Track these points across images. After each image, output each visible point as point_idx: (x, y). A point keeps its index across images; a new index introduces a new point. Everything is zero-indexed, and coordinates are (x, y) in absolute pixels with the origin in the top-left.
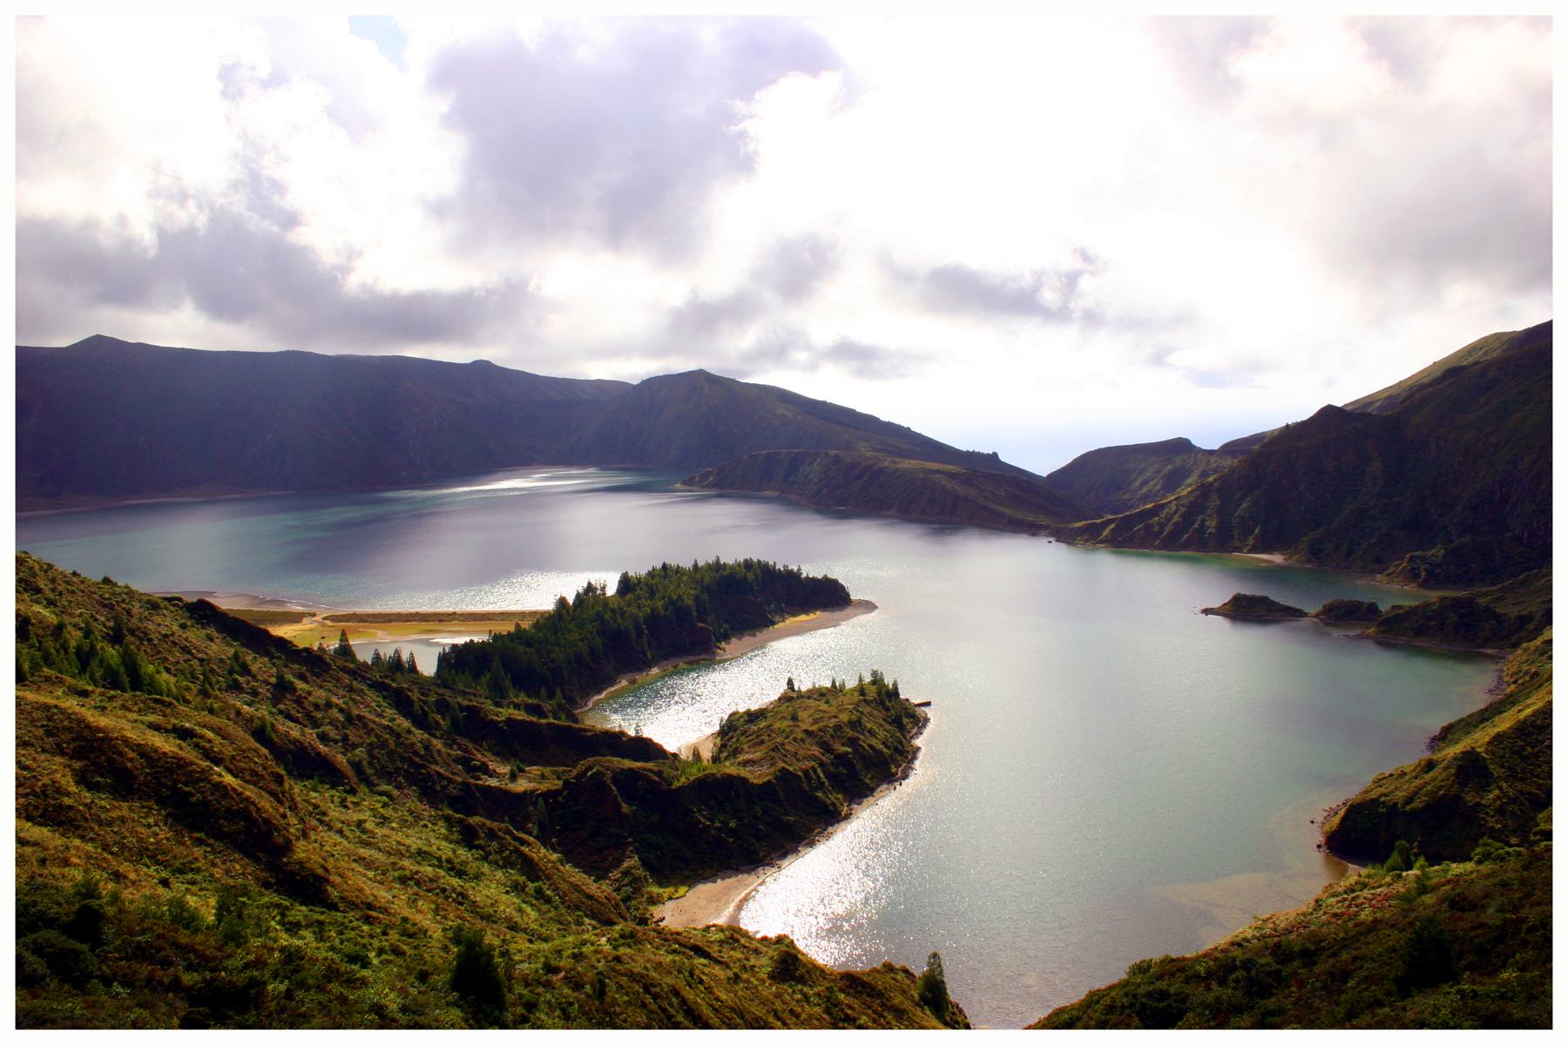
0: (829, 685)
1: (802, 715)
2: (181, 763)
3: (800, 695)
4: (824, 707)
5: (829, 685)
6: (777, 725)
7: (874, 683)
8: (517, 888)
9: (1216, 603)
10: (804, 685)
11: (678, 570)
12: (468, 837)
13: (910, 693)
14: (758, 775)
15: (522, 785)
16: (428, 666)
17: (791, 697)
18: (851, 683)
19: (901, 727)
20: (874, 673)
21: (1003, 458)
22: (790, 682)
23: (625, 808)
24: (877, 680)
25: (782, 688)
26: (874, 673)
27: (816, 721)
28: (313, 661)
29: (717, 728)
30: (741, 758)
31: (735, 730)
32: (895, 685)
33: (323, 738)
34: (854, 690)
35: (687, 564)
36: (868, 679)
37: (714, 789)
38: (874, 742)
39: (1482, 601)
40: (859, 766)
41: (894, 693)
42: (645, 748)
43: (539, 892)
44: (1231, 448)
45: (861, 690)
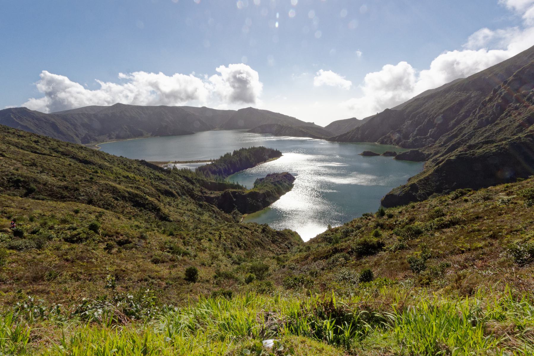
2: (137, 195)
8: (210, 216)
9: (360, 153)
11: (246, 149)
12: (201, 206)
15: (212, 196)
16: (194, 171)
21: (315, 124)
23: (235, 200)
28: (168, 172)
33: (170, 188)
35: (247, 148)
37: (253, 195)
39: (420, 151)
43: (216, 217)
44: (364, 119)
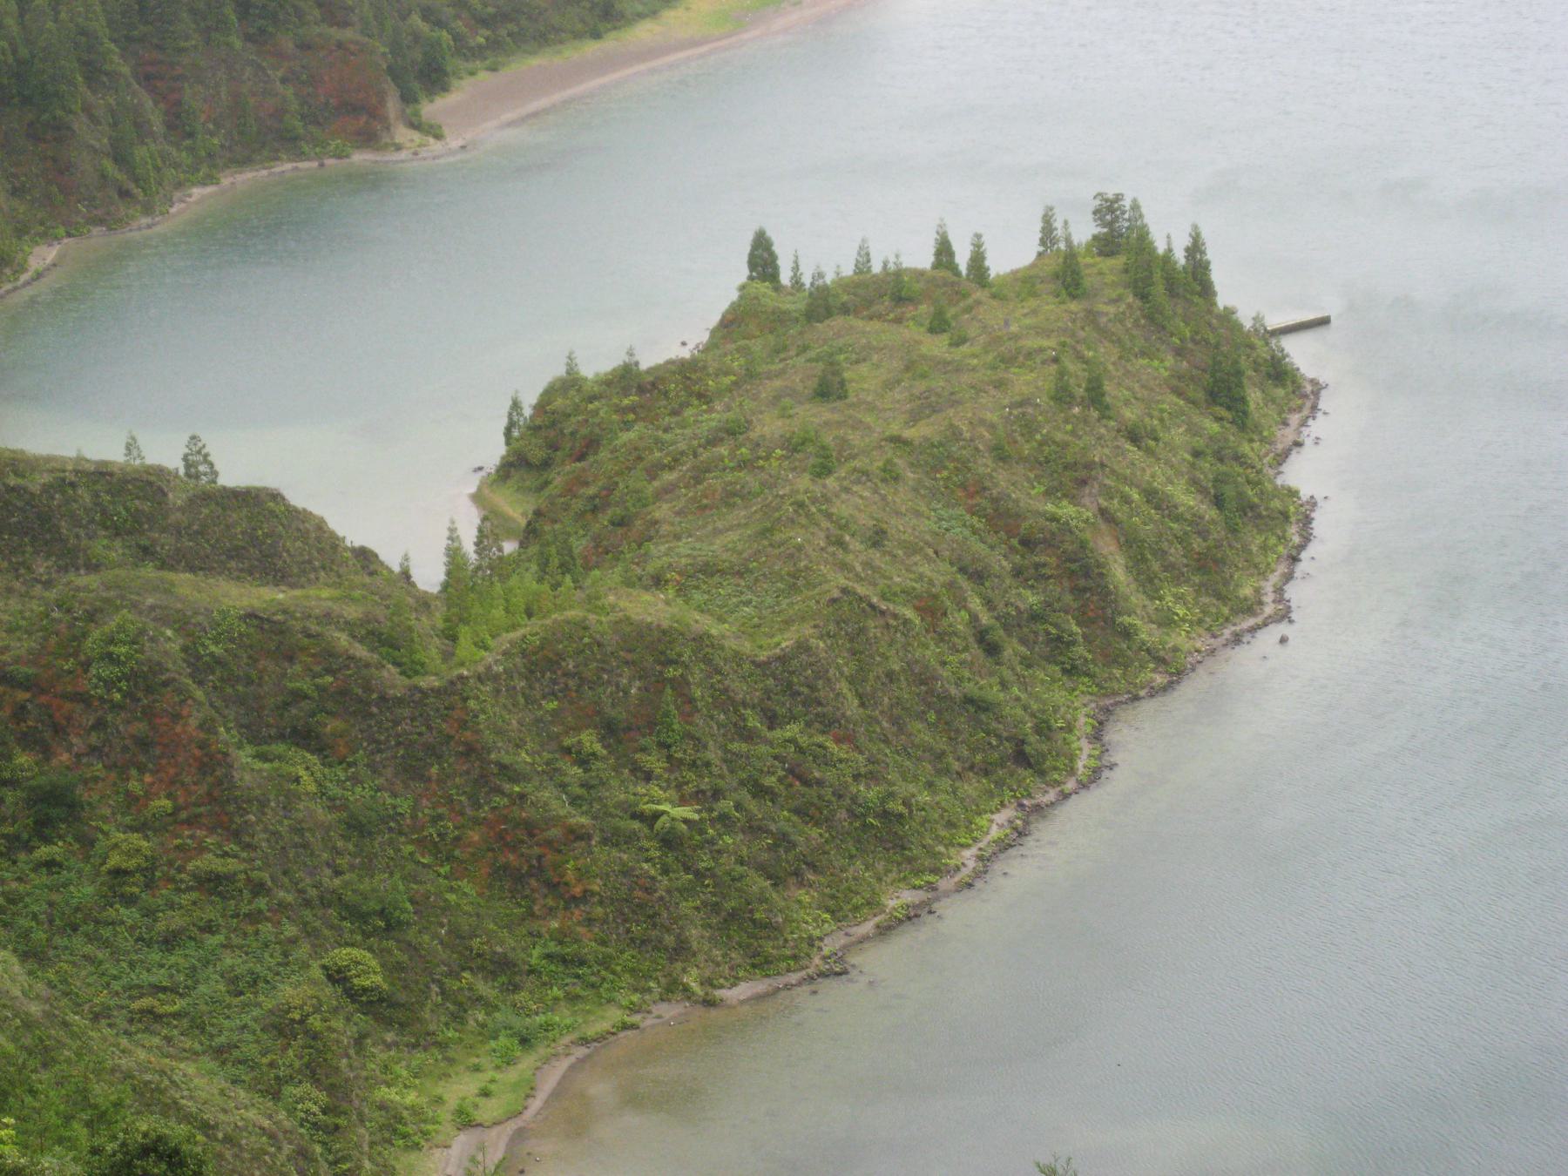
0: (921, 258)
1: (863, 379)
3: (823, 303)
4: (936, 346)
5: (921, 258)
6: (769, 426)
7: (1107, 245)
10: (819, 253)
13: (1243, 293)
14: (739, 628)
17: (776, 316)
18: (1012, 254)
19: (1241, 419)
20: (1108, 209)
22: (762, 259)
24: (1120, 234)
25: (722, 284)
26: (1108, 209)
27: (925, 407)
29: (494, 451)
30: (659, 555)
31: (572, 454)
32: (1196, 248)
34: (1025, 283)
36: (1083, 231)
38: (1157, 474)
40: (1119, 573)
41: (1193, 279)
42: (260, 532)
45: (1062, 273)
